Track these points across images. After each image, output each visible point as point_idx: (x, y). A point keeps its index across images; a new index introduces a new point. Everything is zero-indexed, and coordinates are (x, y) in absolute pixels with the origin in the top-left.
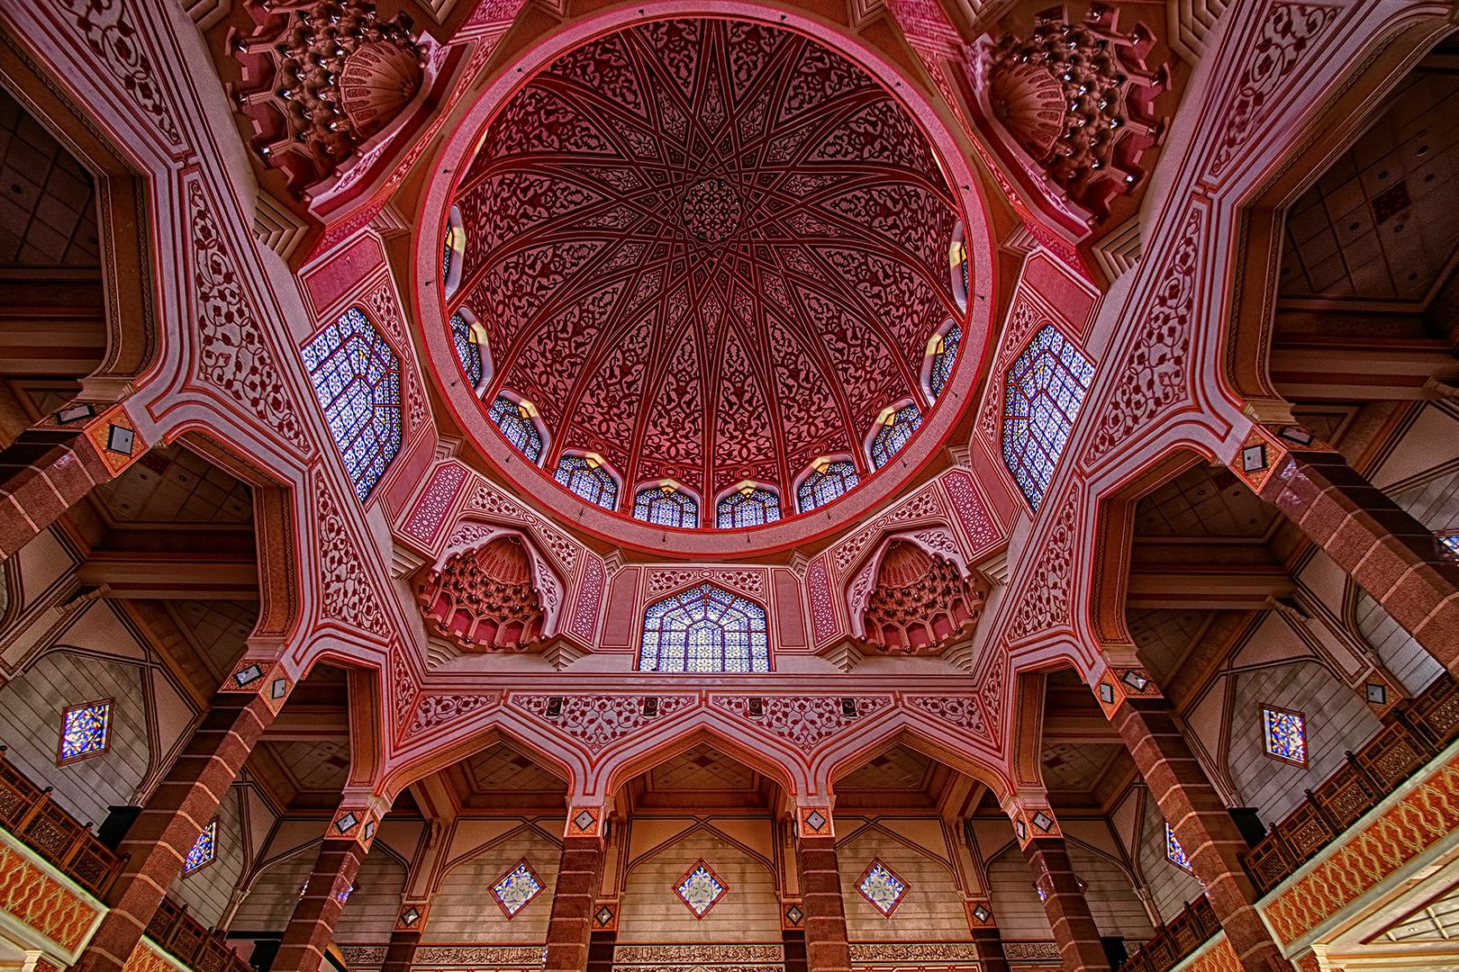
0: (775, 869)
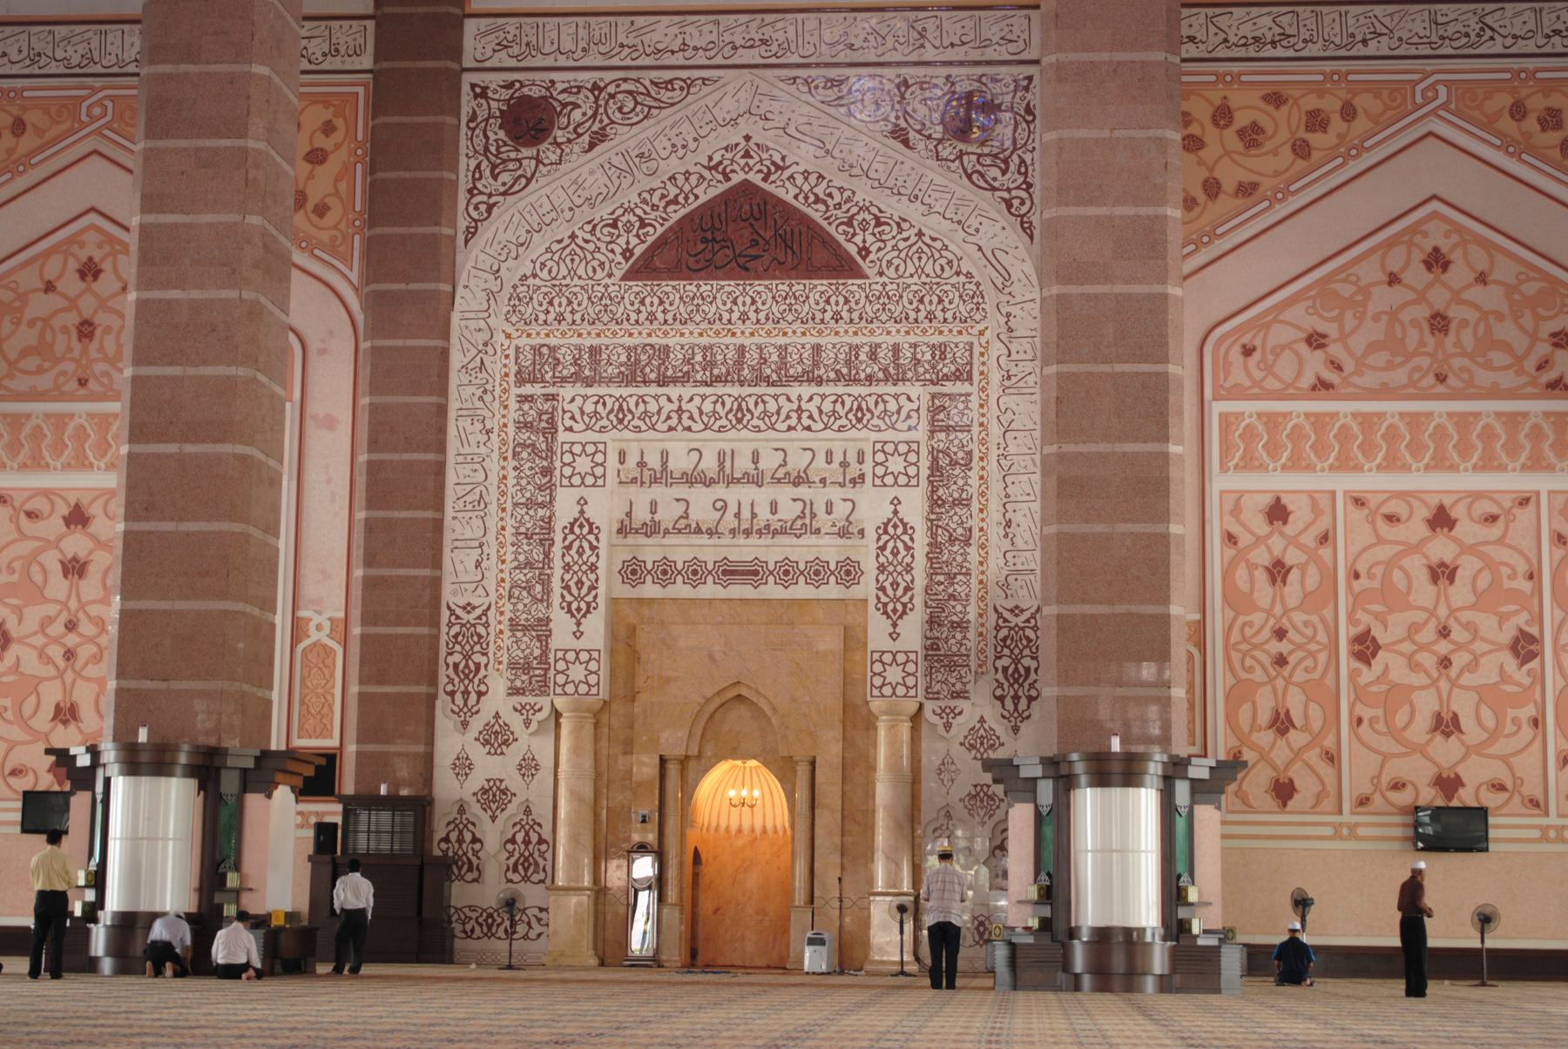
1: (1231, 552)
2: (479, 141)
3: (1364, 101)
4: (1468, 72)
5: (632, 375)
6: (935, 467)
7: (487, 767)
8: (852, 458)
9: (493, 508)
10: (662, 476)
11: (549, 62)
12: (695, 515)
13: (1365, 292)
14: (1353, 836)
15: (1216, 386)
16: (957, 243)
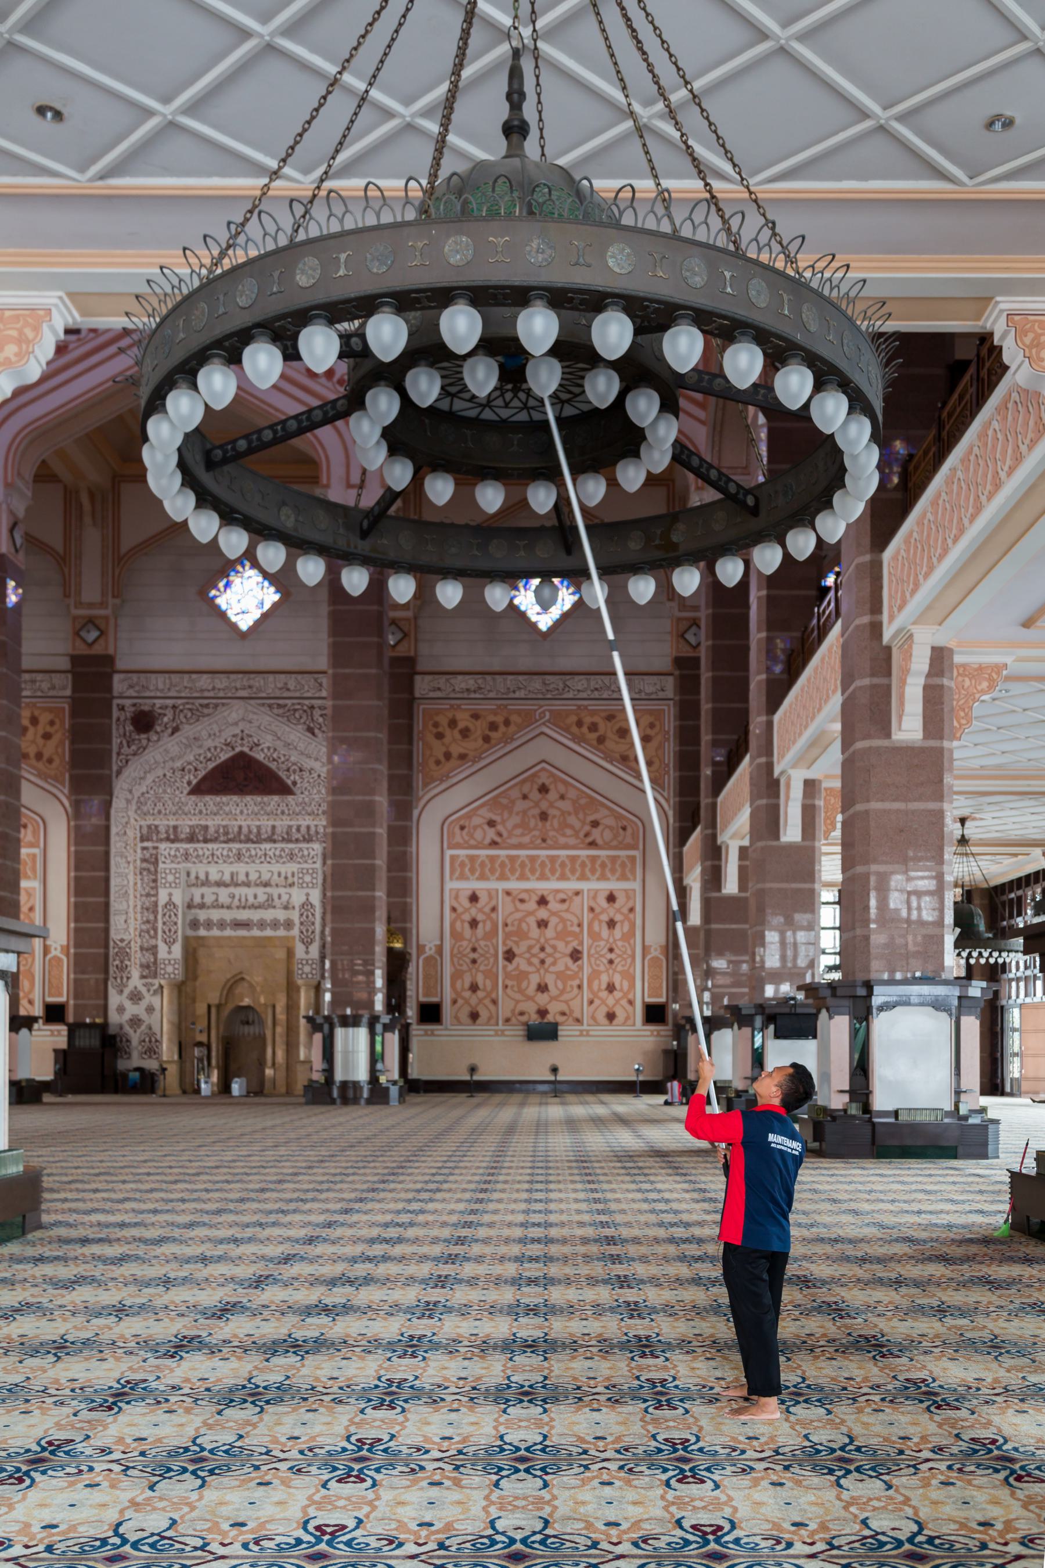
1: (454, 915)
2: (121, 731)
3: (514, 718)
4: (558, 706)
5: (191, 839)
8: (289, 875)
9: (132, 897)
10: (206, 883)
11: (152, 694)
12: (221, 900)
13: (513, 802)
14: (503, 1035)
15: (449, 843)
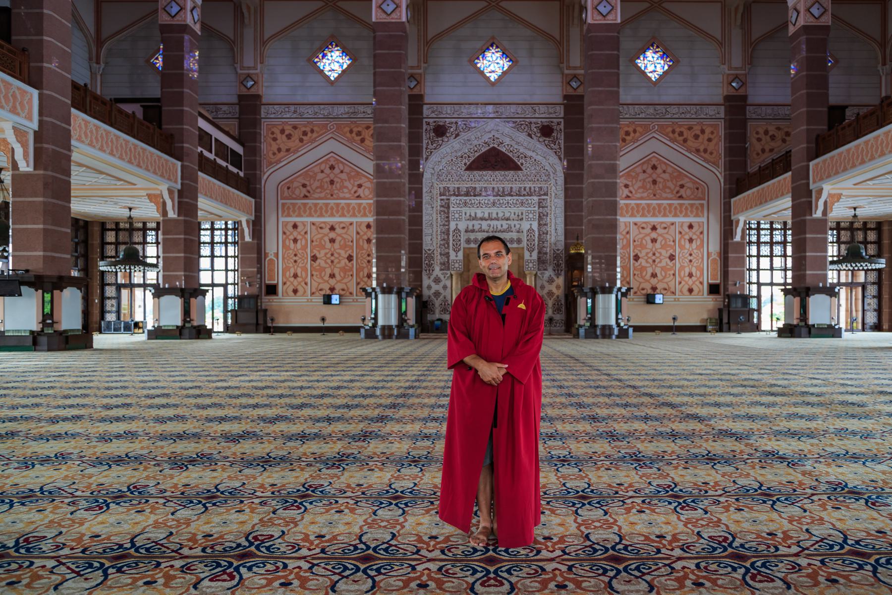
0: (560, 45)
3: (638, 129)
4: (662, 122)
6: (539, 216)
7: (435, 288)
10: (475, 218)
13: (638, 174)
16: (544, 162)
